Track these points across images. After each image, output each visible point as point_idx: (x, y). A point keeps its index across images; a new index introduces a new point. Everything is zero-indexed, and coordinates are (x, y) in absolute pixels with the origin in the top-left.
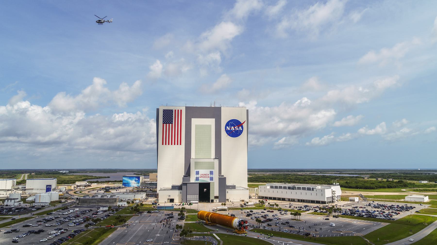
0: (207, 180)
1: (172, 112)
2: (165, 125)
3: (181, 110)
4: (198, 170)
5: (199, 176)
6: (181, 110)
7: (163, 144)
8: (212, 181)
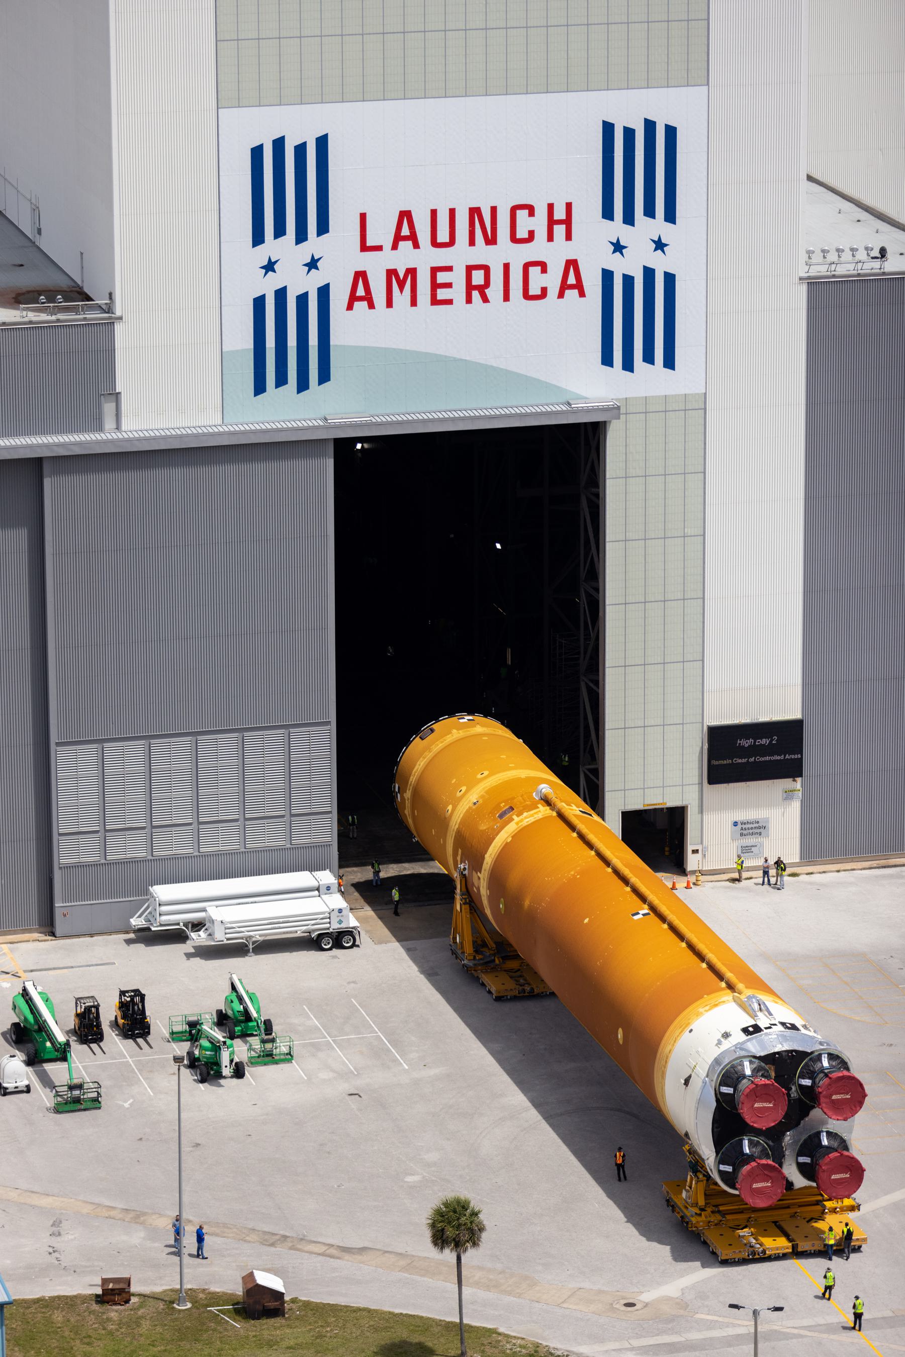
0: (525, 362)
5: (338, 256)
8: (649, 380)
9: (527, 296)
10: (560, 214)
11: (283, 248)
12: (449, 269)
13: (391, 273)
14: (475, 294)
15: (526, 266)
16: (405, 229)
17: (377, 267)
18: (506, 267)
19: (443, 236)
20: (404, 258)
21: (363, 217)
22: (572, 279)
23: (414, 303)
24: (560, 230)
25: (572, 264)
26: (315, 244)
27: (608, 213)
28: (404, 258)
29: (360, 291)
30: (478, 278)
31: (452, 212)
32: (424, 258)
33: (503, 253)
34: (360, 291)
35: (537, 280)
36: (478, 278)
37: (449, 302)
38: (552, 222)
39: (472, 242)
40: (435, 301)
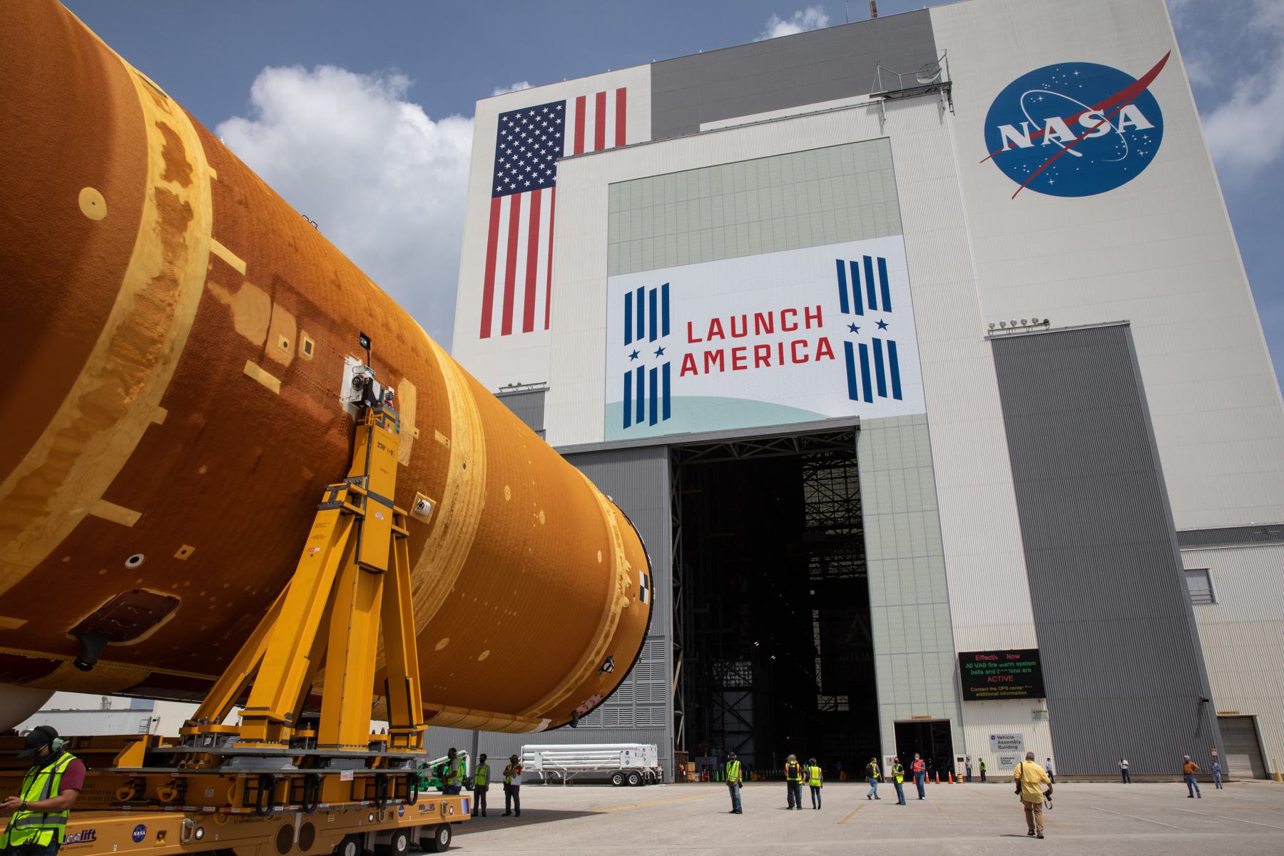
1: (562, 114)
2: (506, 201)
3: (621, 94)
4: (652, 280)
6: (621, 94)
7: (485, 332)
9: (795, 360)
10: (813, 312)
11: (644, 346)
12: (744, 348)
13: (707, 354)
14: (761, 362)
15: (794, 344)
16: (715, 328)
17: (698, 351)
18: (781, 345)
19: (739, 330)
20: (715, 344)
21: (690, 324)
22: (824, 348)
23: (722, 369)
24: (814, 322)
25: (824, 340)
26: (661, 341)
27: (845, 309)
28: (715, 344)
29: (689, 364)
30: (763, 352)
31: (744, 317)
32: (728, 344)
33: (778, 336)
34: (689, 364)
35: (801, 351)
36: (763, 352)
37: (745, 367)
38: (808, 318)
39: (758, 332)
40: (735, 368)
